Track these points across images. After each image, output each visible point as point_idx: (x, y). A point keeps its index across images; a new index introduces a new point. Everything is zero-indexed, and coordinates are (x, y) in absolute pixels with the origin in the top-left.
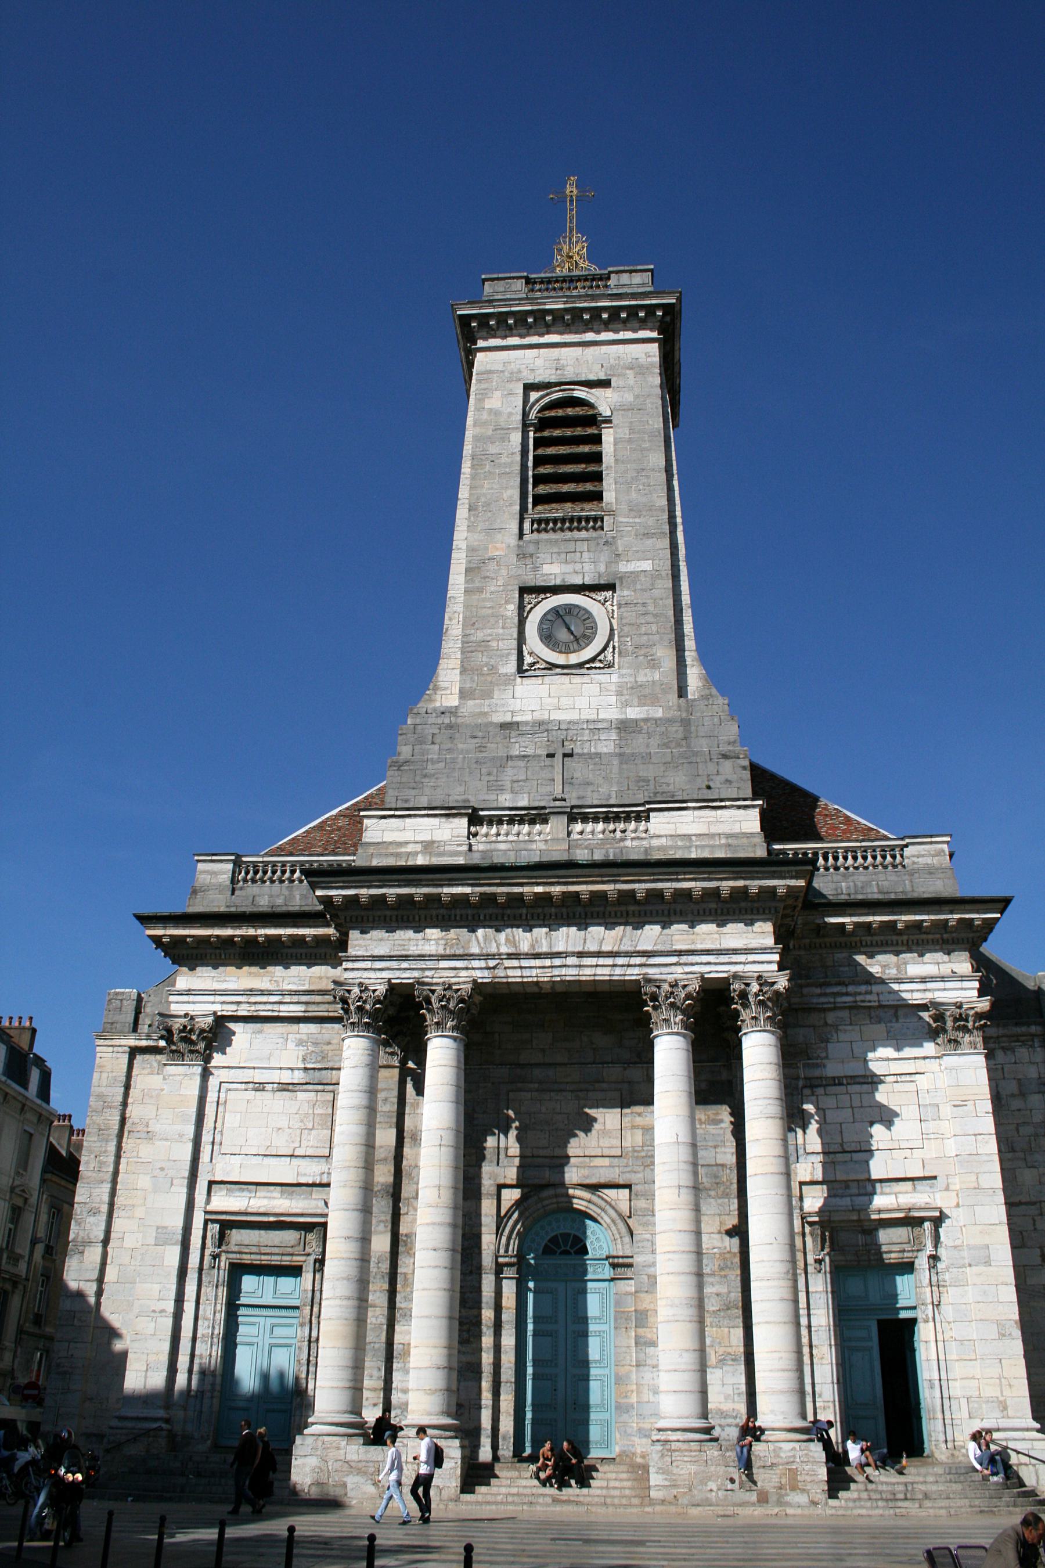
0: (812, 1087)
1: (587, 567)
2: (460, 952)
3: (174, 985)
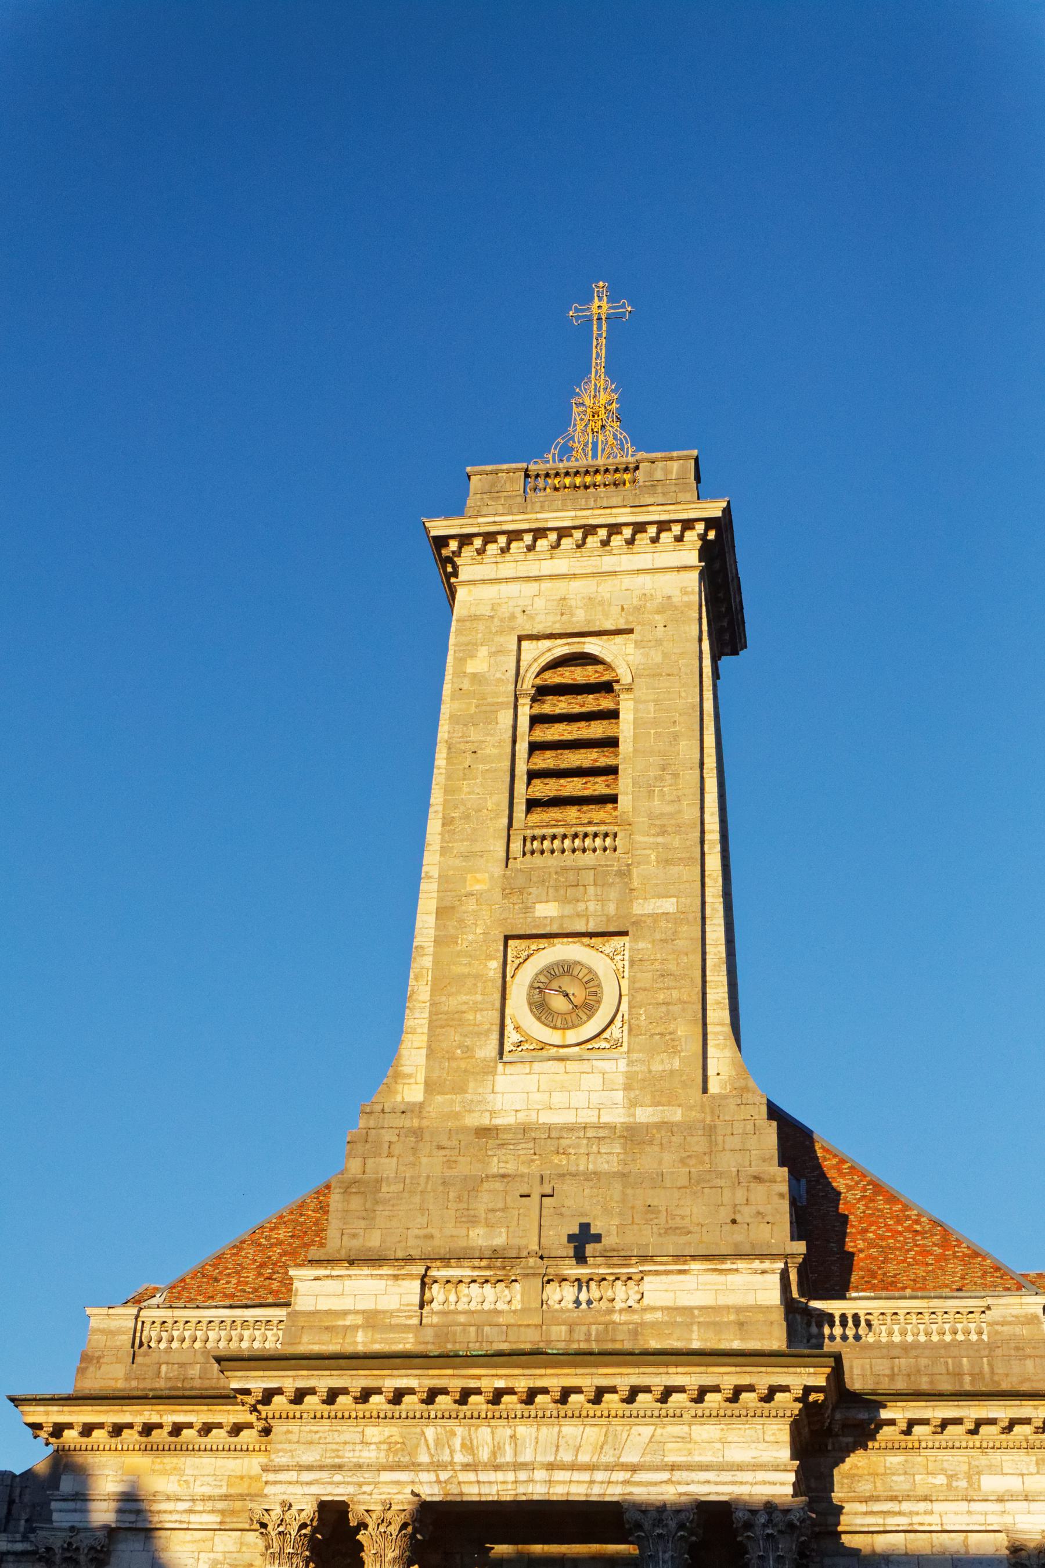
1: (592, 906)
3: (58, 1489)
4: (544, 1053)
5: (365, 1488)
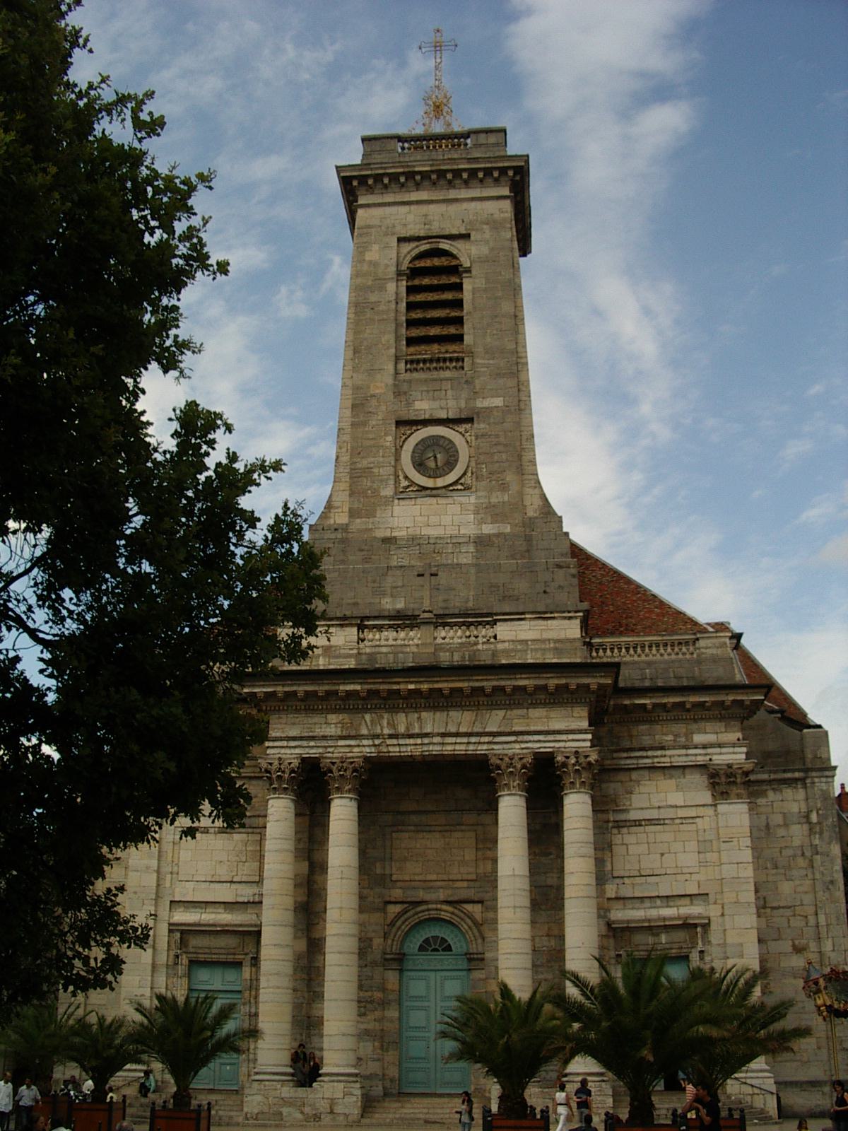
0: (618, 827)
1: (451, 403)
2: (353, 733)
4: (423, 493)
5: (330, 750)
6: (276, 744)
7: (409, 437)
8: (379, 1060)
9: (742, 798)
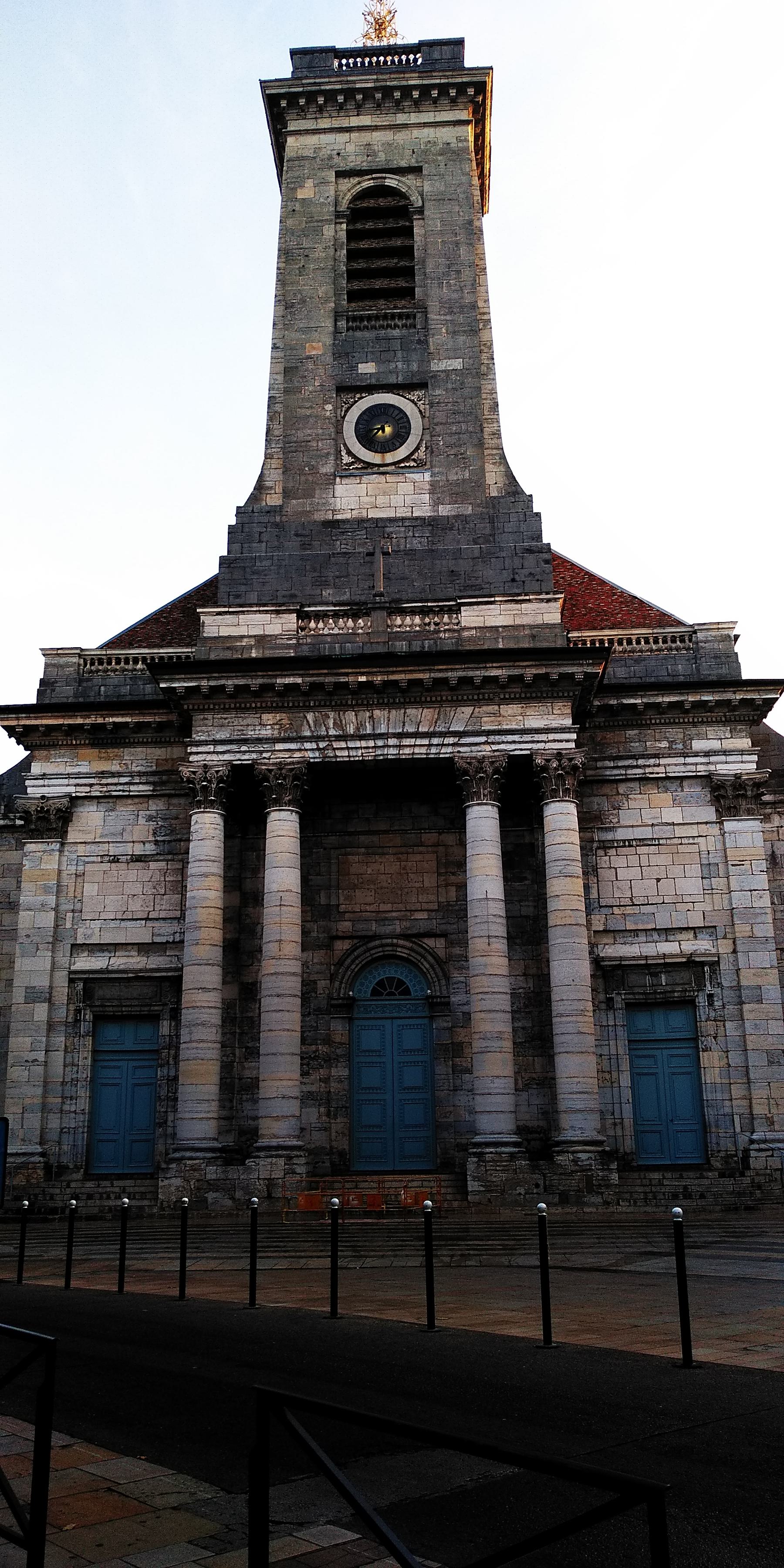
1: (400, 365)
4: (370, 471)
5: (264, 755)
6: (200, 749)
7: (352, 406)
8: (325, 1129)
9: (753, 814)
